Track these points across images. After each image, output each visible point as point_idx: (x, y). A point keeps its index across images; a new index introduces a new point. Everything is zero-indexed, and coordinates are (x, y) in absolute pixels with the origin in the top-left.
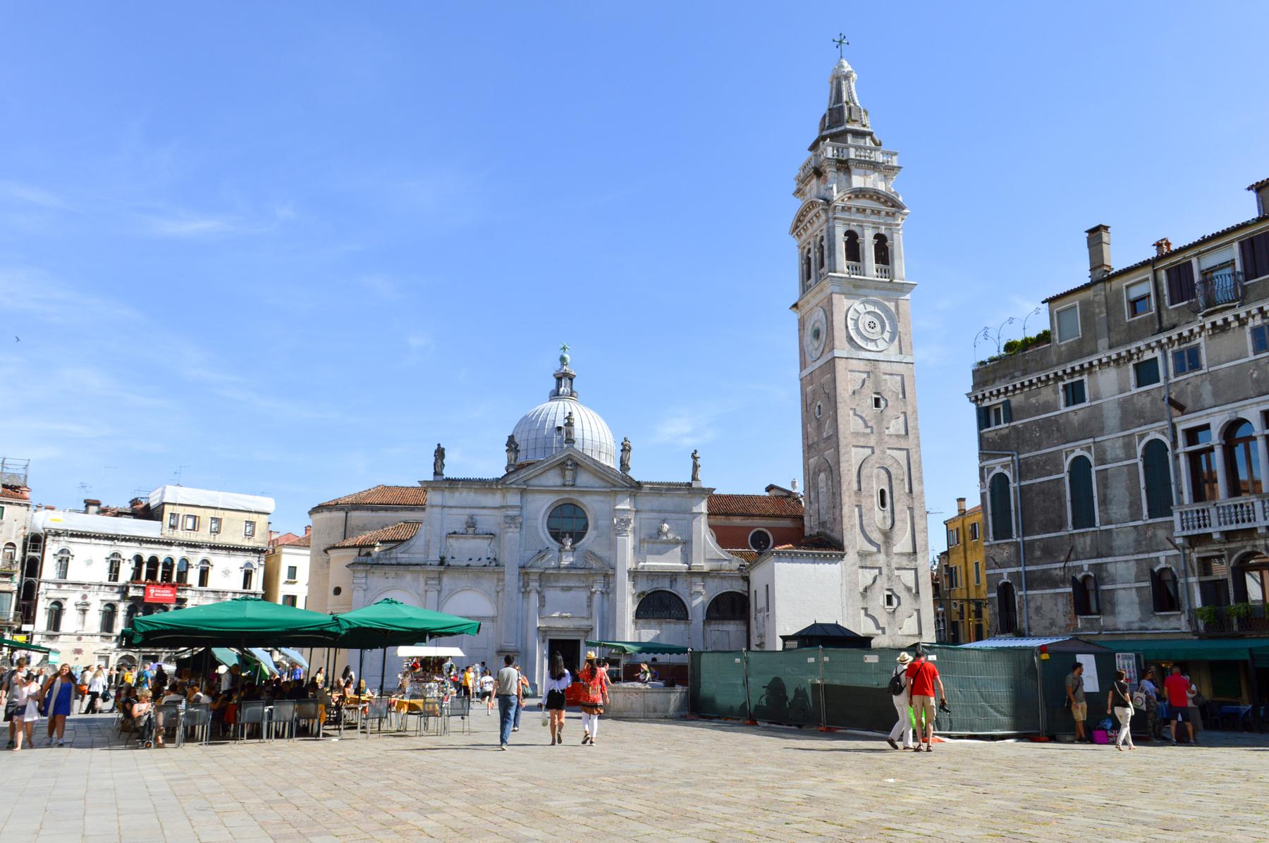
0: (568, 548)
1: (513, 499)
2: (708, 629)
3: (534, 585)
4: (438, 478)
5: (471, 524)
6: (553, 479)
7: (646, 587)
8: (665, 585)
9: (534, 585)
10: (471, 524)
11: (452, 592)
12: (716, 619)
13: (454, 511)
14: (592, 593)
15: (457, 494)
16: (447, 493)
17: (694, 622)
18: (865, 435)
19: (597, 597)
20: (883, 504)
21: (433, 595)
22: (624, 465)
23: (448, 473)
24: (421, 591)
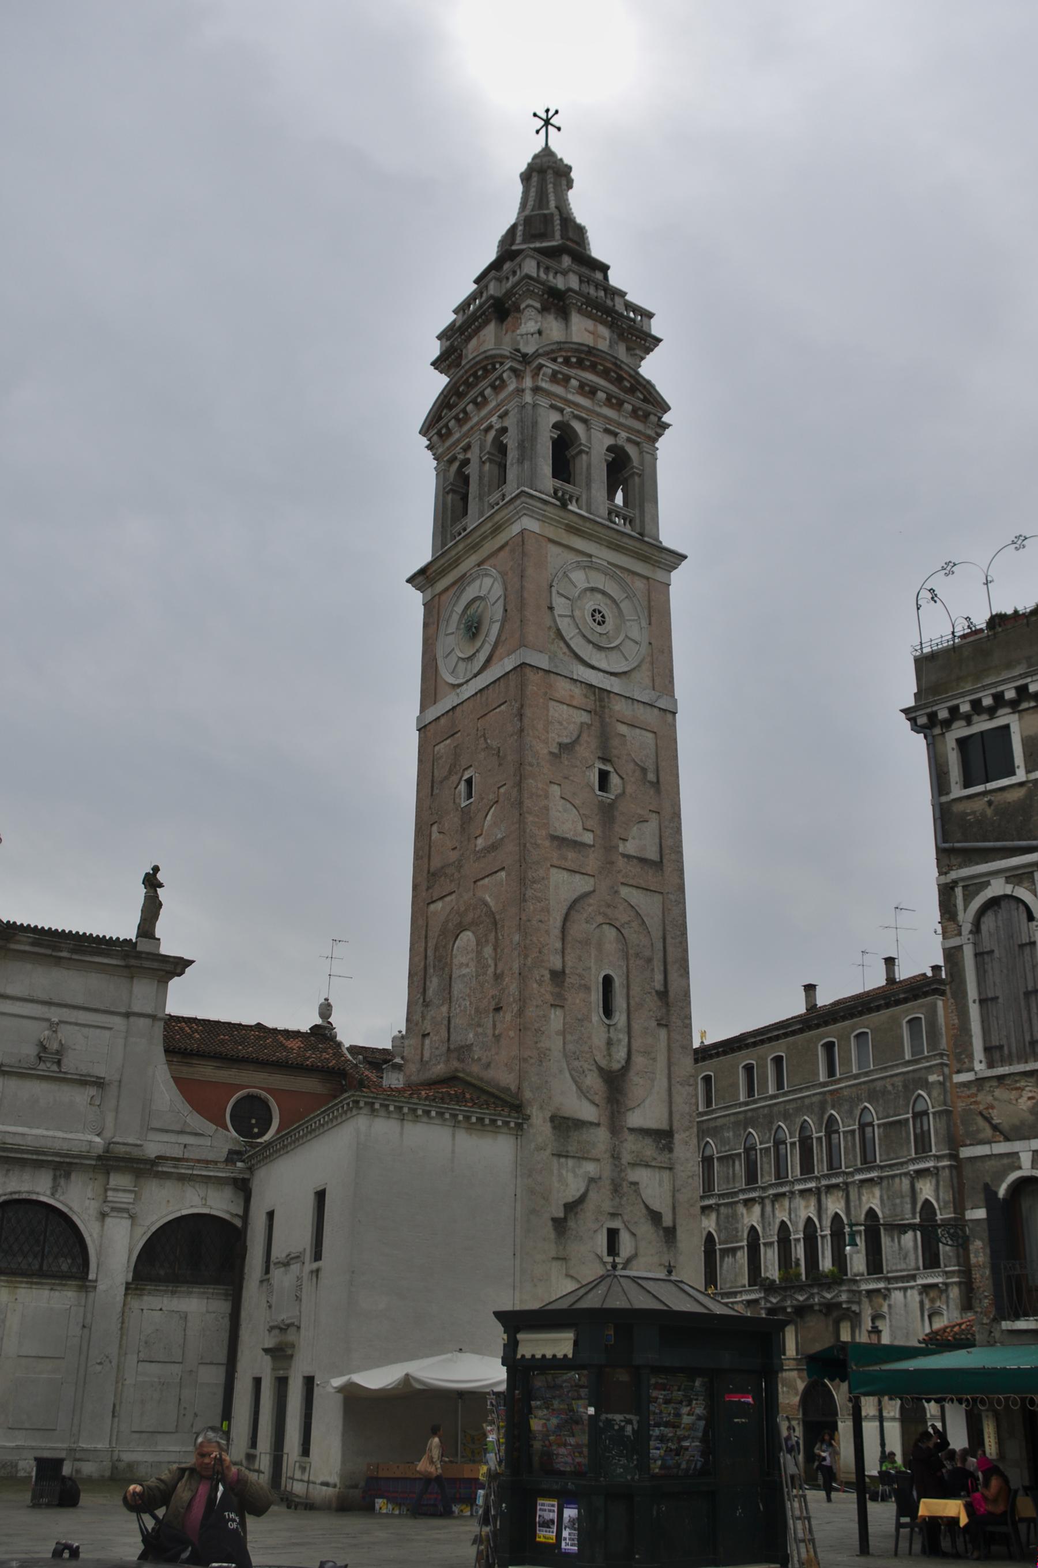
2: (135, 1304)
8: (37, 1187)
12: (156, 1280)
18: (577, 845)
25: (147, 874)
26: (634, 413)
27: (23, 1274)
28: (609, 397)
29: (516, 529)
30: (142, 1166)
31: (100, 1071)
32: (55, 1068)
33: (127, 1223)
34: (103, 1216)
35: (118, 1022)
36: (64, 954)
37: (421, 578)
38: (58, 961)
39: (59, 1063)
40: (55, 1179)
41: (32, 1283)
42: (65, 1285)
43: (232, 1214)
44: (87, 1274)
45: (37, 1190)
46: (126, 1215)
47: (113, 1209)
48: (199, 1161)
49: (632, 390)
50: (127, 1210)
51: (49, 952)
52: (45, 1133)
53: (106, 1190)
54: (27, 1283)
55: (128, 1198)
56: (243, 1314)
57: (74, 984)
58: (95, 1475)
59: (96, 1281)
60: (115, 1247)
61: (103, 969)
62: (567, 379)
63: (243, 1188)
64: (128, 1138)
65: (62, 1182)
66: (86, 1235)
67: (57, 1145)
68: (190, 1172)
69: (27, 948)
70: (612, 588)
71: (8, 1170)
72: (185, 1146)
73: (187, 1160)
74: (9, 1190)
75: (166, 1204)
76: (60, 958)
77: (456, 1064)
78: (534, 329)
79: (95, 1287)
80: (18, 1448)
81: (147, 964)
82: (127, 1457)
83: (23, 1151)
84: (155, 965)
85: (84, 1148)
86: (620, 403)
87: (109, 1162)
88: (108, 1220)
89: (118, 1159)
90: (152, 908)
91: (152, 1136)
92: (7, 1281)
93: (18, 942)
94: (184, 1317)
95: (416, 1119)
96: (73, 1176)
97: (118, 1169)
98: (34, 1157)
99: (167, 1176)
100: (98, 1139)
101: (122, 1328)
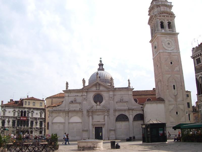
0: (98, 105)
6: (94, 89)
7: (117, 114)
8: (123, 113)
11: (72, 117)
12: (136, 120)
13: (71, 97)
14: (105, 116)
16: (69, 93)
19: (106, 117)
20: (174, 89)
21: (67, 117)
23: (69, 88)
26: (170, 17)
28: (167, 16)
29: (157, 36)
34: (129, 115)
37: (151, 42)
49: (170, 14)
57: (122, 93)
60: (131, 118)
62: (161, 16)
63: (143, 110)
64: (131, 107)
66: (128, 117)
70: (171, 40)
75: (135, 113)
77: (160, 96)
78: (156, 10)
85: (126, 109)
86: (168, 16)
87: (129, 109)
90: (129, 83)
94: (139, 124)
95: (153, 104)
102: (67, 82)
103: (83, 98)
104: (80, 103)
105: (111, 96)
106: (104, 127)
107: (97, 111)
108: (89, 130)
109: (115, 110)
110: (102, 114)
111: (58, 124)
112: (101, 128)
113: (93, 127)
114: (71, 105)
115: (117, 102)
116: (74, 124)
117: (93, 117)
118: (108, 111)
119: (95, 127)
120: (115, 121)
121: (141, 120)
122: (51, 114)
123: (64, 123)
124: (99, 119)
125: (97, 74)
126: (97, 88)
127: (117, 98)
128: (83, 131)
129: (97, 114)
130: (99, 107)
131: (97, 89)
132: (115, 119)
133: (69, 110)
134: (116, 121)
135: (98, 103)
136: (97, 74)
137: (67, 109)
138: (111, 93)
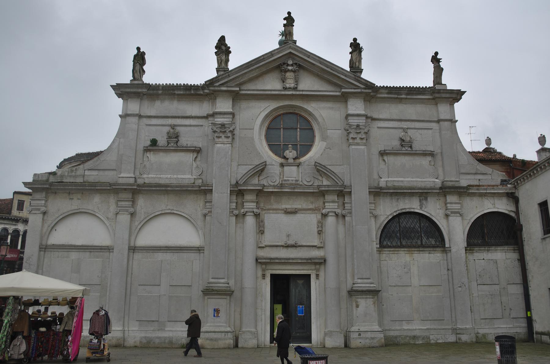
1: (224, 105)
2: (471, 257)
3: (250, 206)
4: (136, 82)
5: (174, 136)
6: (272, 84)
7: (387, 209)
8: (413, 205)
9: (250, 206)
10: (174, 136)
13: (154, 121)
14: (325, 216)
15: (158, 103)
16: (146, 103)
17: (453, 250)
19: (331, 220)
21: (124, 218)
22: (356, 66)
23: (148, 78)
24: (111, 215)
25: (433, 56)
27: (415, 247)
30: (462, 190)
31: (431, 148)
32: (409, 149)
33: (459, 219)
34: (447, 216)
35: (434, 125)
36: (403, 96)
38: (400, 100)
39: (411, 147)
40: (420, 201)
41: (419, 251)
42: (435, 251)
43: (508, 211)
44: (445, 245)
45: (413, 207)
46: (458, 215)
47: (452, 212)
48: (489, 186)
50: (458, 213)
51: (396, 96)
52: (412, 179)
53: (446, 204)
54: (417, 251)
55: (457, 206)
56: (528, 258)
57: (411, 110)
58: (469, 341)
59: (450, 247)
60: (456, 231)
61: (422, 101)
63: (513, 198)
64: (452, 178)
65: (424, 202)
66: (440, 226)
67: (419, 185)
68: (485, 191)
69: (386, 96)
71: (398, 199)
72: (479, 180)
73: (483, 186)
74: (400, 208)
76: (402, 99)
79: (450, 251)
80: (428, 329)
81: (444, 95)
82: (482, 331)
83: (404, 189)
84: (448, 95)
87: (445, 190)
88: (450, 218)
89: (450, 188)
90: (438, 71)
91: (462, 177)
92: (408, 251)
93: (382, 93)
94: (496, 262)
96: (429, 199)
97: (450, 193)
98: (410, 191)
99: (474, 194)
100: (437, 180)
101: (467, 270)
102: (138, 49)
103: (214, 124)
104: (198, 151)
105: (354, 121)
106: (317, 276)
107: (283, 192)
108: (242, 289)
109: (377, 192)
110: (311, 206)
111: (74, 255)
112: (300, 282)
113: (260, 273)
114: (152, 157)
115: (383, 154)
116: (160, 256)
117: (262, 221)
118: (343, 193)
119: (272, 276)
120: (375, 245)
121: (507, 244)
122: (43, 202)
123: (109, 249)
124: (291, 229)
125: (285, 22)
126: (289, 81)
127: (384, 136)
128: (208, 292)
129: (288, 206)
130: (292, 173)
131: (288, 86)
132: (375, 235)
133: (140, 181)
134: (382, 246)
135: (290, 154)
136: (285, 22)
137: (126, 176)
138: (356, 107)
